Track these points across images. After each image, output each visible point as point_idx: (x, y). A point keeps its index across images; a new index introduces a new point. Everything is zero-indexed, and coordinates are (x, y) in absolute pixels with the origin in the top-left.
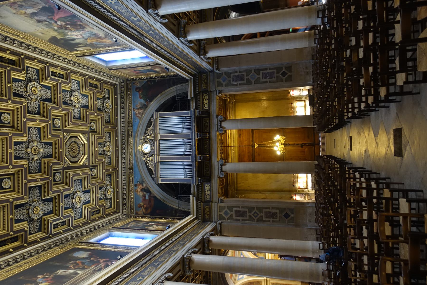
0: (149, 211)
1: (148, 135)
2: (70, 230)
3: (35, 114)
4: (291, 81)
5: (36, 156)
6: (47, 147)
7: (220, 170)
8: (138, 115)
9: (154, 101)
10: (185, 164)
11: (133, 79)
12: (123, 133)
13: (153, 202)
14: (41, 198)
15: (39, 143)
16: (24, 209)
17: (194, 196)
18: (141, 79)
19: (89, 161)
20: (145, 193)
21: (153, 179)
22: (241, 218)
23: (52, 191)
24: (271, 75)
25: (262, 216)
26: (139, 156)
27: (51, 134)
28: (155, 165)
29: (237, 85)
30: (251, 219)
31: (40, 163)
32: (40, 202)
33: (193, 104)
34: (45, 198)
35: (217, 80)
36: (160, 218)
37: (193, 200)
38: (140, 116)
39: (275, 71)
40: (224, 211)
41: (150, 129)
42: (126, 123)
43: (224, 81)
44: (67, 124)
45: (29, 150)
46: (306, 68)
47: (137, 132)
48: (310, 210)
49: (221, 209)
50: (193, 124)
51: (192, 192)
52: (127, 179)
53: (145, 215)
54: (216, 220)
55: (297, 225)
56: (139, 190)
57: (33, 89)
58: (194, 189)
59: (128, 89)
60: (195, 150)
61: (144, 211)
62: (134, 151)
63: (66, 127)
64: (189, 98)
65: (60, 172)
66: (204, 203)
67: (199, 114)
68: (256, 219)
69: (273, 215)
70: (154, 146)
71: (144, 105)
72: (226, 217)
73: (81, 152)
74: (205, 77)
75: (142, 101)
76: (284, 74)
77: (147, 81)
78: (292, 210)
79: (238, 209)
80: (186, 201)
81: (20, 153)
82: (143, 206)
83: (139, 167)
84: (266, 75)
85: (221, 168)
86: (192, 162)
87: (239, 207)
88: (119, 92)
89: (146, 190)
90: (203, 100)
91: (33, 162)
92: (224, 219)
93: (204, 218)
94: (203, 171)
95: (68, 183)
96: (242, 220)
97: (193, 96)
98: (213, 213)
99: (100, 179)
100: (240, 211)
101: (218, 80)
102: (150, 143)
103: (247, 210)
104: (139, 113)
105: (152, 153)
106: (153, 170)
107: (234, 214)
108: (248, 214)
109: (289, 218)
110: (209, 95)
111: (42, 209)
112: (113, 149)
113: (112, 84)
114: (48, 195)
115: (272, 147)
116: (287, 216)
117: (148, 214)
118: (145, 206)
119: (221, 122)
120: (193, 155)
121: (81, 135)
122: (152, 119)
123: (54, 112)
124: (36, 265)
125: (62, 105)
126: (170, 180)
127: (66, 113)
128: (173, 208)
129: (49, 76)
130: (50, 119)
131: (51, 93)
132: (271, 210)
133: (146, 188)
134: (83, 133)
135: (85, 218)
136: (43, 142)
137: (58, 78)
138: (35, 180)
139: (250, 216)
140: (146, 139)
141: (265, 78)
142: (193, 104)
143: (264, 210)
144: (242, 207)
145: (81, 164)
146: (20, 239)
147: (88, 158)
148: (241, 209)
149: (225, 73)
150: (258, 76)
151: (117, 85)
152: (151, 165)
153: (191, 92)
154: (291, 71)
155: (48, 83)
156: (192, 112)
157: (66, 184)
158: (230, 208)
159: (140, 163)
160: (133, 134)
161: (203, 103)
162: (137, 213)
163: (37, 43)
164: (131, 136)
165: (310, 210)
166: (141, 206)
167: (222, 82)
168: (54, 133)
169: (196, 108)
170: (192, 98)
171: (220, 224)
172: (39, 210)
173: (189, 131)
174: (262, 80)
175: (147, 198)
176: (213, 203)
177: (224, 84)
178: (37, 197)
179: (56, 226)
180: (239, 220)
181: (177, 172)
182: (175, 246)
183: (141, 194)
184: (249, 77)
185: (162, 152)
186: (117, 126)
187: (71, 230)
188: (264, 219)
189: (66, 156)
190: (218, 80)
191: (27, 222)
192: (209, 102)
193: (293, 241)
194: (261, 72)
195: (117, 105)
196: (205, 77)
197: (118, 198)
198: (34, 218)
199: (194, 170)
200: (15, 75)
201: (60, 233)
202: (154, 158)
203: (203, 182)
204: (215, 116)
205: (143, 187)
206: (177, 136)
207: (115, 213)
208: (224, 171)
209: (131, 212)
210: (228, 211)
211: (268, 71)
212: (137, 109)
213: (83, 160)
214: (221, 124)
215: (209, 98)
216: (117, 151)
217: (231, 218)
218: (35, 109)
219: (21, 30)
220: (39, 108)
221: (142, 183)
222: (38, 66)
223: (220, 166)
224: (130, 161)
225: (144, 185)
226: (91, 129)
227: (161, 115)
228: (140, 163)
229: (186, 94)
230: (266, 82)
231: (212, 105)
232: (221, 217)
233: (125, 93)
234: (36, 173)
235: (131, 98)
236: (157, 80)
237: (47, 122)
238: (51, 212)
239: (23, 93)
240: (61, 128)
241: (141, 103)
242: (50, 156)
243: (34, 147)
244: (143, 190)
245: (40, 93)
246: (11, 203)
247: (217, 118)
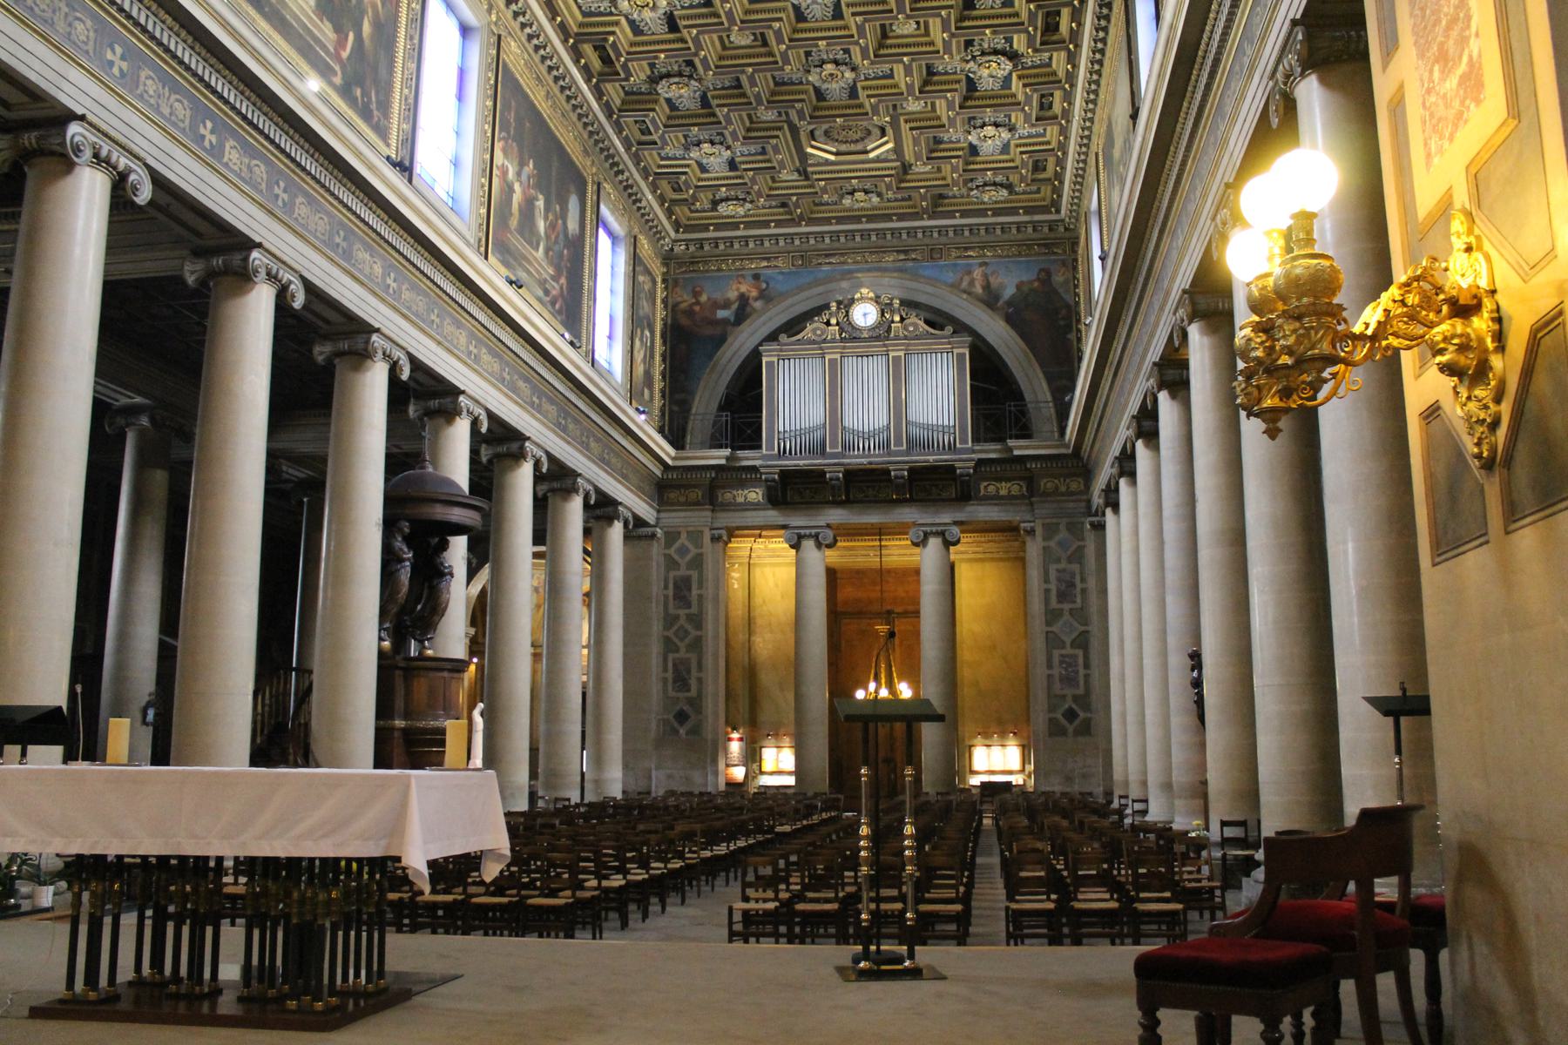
0: (684, 321)
1: (902, 320)
2: (628, 147)
4: (1051, 734)
8: (966, 279)
9: (1008, 328)
10: (818, 434)
11: (1076, 260)
12: (911, 232)
13: (708, 331)
17: (728, 459)
18: (1076, 286)
19: (819, 164)
20: (735, 306)
21: (772, 337)
22: (671, 592)
24: (1069, 680)
25: (677, 651)
26: (844, 284)
28: (814, 342)
29: (1047, 581)
30: (670, 621)
33: (994, 451)
35: (1065, 521)
36: (664, 356)
37: (718, 456)
38: (964, 284)
39: (1081, 691)
40: (687, 543)
41: (921, 323)
42: (943, 240)
43: (1060, 544)
46: (1084, 776)
47: (915, 276)
48: (697, 777)
49: (695, 536)
50: (931, 458)
51: (740, 453)
52: (775, 249)
53: (671, 307)
54: (664, 522)
55: (659, 743)
56: (743, 288)
58: (748, 458)
59: (1048, 246)
60: (856, 460)
61: (683, 306)
62: (858, 271)
64: (1011, 443)
66: (709, 490)
67: (962, 475)
68: (670, 633)
69: (681, 681)
70: (872, 339)
71: (997, 297)
72: (672, 551)
73: (843, 148)
74: (1074, 486)
75: (1009, 292)
76: (1071, 715)
77: (1068, 306)
78: (696, 731)
79: (694, 586)
80: (713, 437)
82: (698, 303)
83: (809, 286)
84: (1070, 665)
85: (810, 536)
86: (823, 453)
87: (700, 586)
88: (1037, 218)
89: (743, 312)
90: (1008, 480)
92: (668, 545)
93: (667, 487)
96: (666, 597)
97: (1016, 453)
98: (682, 514)
99: (771, 189)
100: (690, 590)
101: (1062, 527)
102: (878, 326)
103: (694, 610)
104: (972, 283)
105: (851, 334)
106: (799, 337)
107: (683, 572)
108: (682, 612)
109: (676, 725)
110: (1022, 497)
112: (862, 209)
115: (877, 679)
116: (682, 717)
117: (674, 319)
118: (697, 308)
119: (942, 534)
120: (844, 457)
121: (890, 146)
122: (949, 329)
126: (771, 389)
128: (692, 393)
132: (694, 673)
133: (748, 309)
134: (898, 150)
135: (660, 167)
139: (677, 617)
140: (893, 312)
141: (1061, 662)
142: (991, 451)
143: (693, 657)
144: (700, 596)
145: (810, 150)
147: (827, 162)
148: (695, 592)
149: (1081, 549)
150: (1068, 641)
151: (1058, 211)
152: (814, 331)
153: (1027, 448)
154: (1077, 733)
156: (969, 453)
159: (821, 289)
160: (910, 264)
161: (1000, 480)
162: (676, 282)
164: (902, 257)
165: (697, 777)
166: (696, 294)
167: (1057, 538)
169: (980, 462)
170: (1010, 450)
171: (653, 535)
172: (683, 93)
173: (912, 444)
174: (1056, 653)
175: (722, 314)
176: (709, 513)
177: (1052, 544)
180: (666, 587)
181: (796, 402)
182: (598, 440)
184: (1066, 616)
185: (851, 364)
186: (930, 218)
188: (671, 656)
190: (1062, 527)
192: (1002, 498)
193: (620, 733)
194: (1080, 653)
195: (994, 215)
196: (1074, 486)
197: (718, 227)
199: (801, 462)
202: (833, 340)
203: (769, 489)
204: (960, 516)
206: (898, 407)
207: (677, 226)
209: (680, 265)
210: (689, 557)
211: (1082, 672)
212: (985, 276)
213: (821, 152)
214: (937, 534)
216: (857, 219)
217: (671, 563)
221: (762, 295)
223: (813, 531)
224: (827, 256)
227: (961, 357)
229: (1025, 433)
230: (1050, 666)
231: (990, 508)
232: (671, 537)
233: (1035, 236)
235: (1020, 255)
241: (1002, 286)
244: (743, 299)
247: (956, 523)
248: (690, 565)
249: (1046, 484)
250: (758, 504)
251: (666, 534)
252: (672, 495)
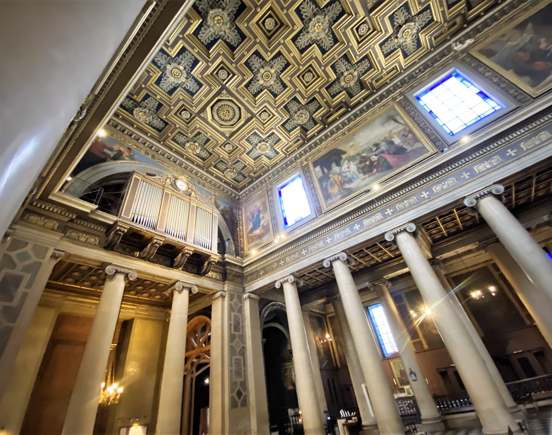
7: (119, 270)
40: (32, 254)
51: (100, 212)
56: (122, 149)
72: (13, 254)
86: (154, 228)
88: (234, 191)
89: (118, 156)
90: (216, 272)
94: (134, 242)
97: (227, 260)
101: (235, 296)
103: (15, 303)
107: (17, 272)
113: (241, 189)
151: (239, 192)
156: (214, 254)
158: (35, 268)
159: (159, 170)
177: (232, 303)
183: (116, 147)
205: (124, 155)
208: (114, 275)
210: (27, 263)
215: (217, 280)
225: (127, 158)
226: (228, 143)
228: (159, 170)
236: (238, 229)
248: (26, 269)
249: (230, 277)
250: (95, 245)
251: (13, 240)
252: (33, 218)
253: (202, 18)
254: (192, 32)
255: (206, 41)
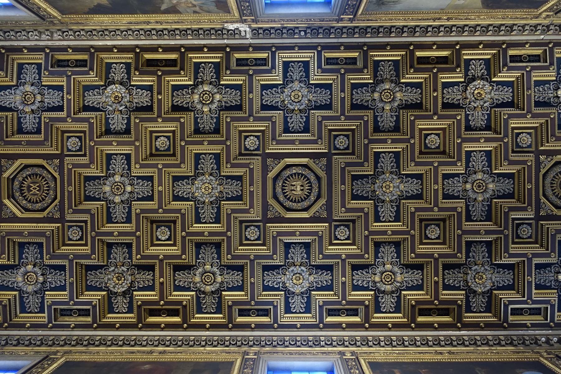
3: (480, 130)
5: (480, 195)
6: (502, 181)
14: (491, 260)
15: (485, 175)
16: (460, 272)
23: (508, 253)
27: (508, 160)
31: (490, 206)
32: (486, 267)
34: (497, 262)
44: (545, 140)
45: (468, 186)
57: (476, 92)
63: (542, 146)
65: (530, 225)
81: (454, 190)
91: (477, 204)
95: (545, 243)
111: (491, 279)
114: (501, 259)
123: (513, 123)
124: (458, 362)
125: (533, 108)
127: (543, 121)
129: (505, 65)
130: (506, 136)
131: (513, 92)
136: (495, 174)
137: (524, 64)
138: (477, 232)
146: (452, 314)
155: (504, 76)
157: (542, 246)
163: (473, 17)
168: (513, 157)
178: (483, 258)
179: (515, 312)
187: (551, 328)
189: (544, 195)
191: (464, 292)
198: (474, 288)
200: (445, 78)
201: (525, 325)
218: (482, 123)
219: (434, 9)
220: (489, 119)
222: (488, 54)
234: (481, 221)
237: (501, 140)
238: (510, 287)
239: (461, 101)
240: (533, 149)
242: (510, 196)
243: (478, 181)
245: (489, 96)
246: (436, 260)
253: (492, 292)
254: (513, 292)
255: (509, 274)
